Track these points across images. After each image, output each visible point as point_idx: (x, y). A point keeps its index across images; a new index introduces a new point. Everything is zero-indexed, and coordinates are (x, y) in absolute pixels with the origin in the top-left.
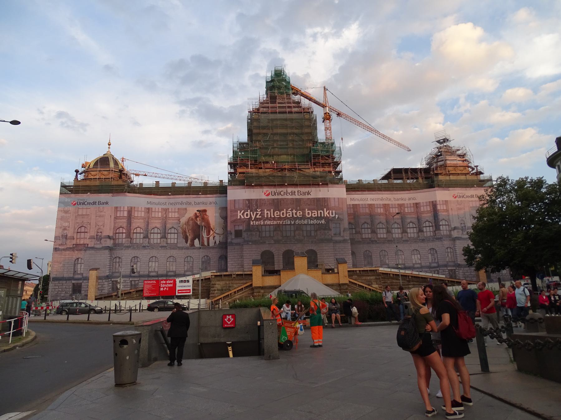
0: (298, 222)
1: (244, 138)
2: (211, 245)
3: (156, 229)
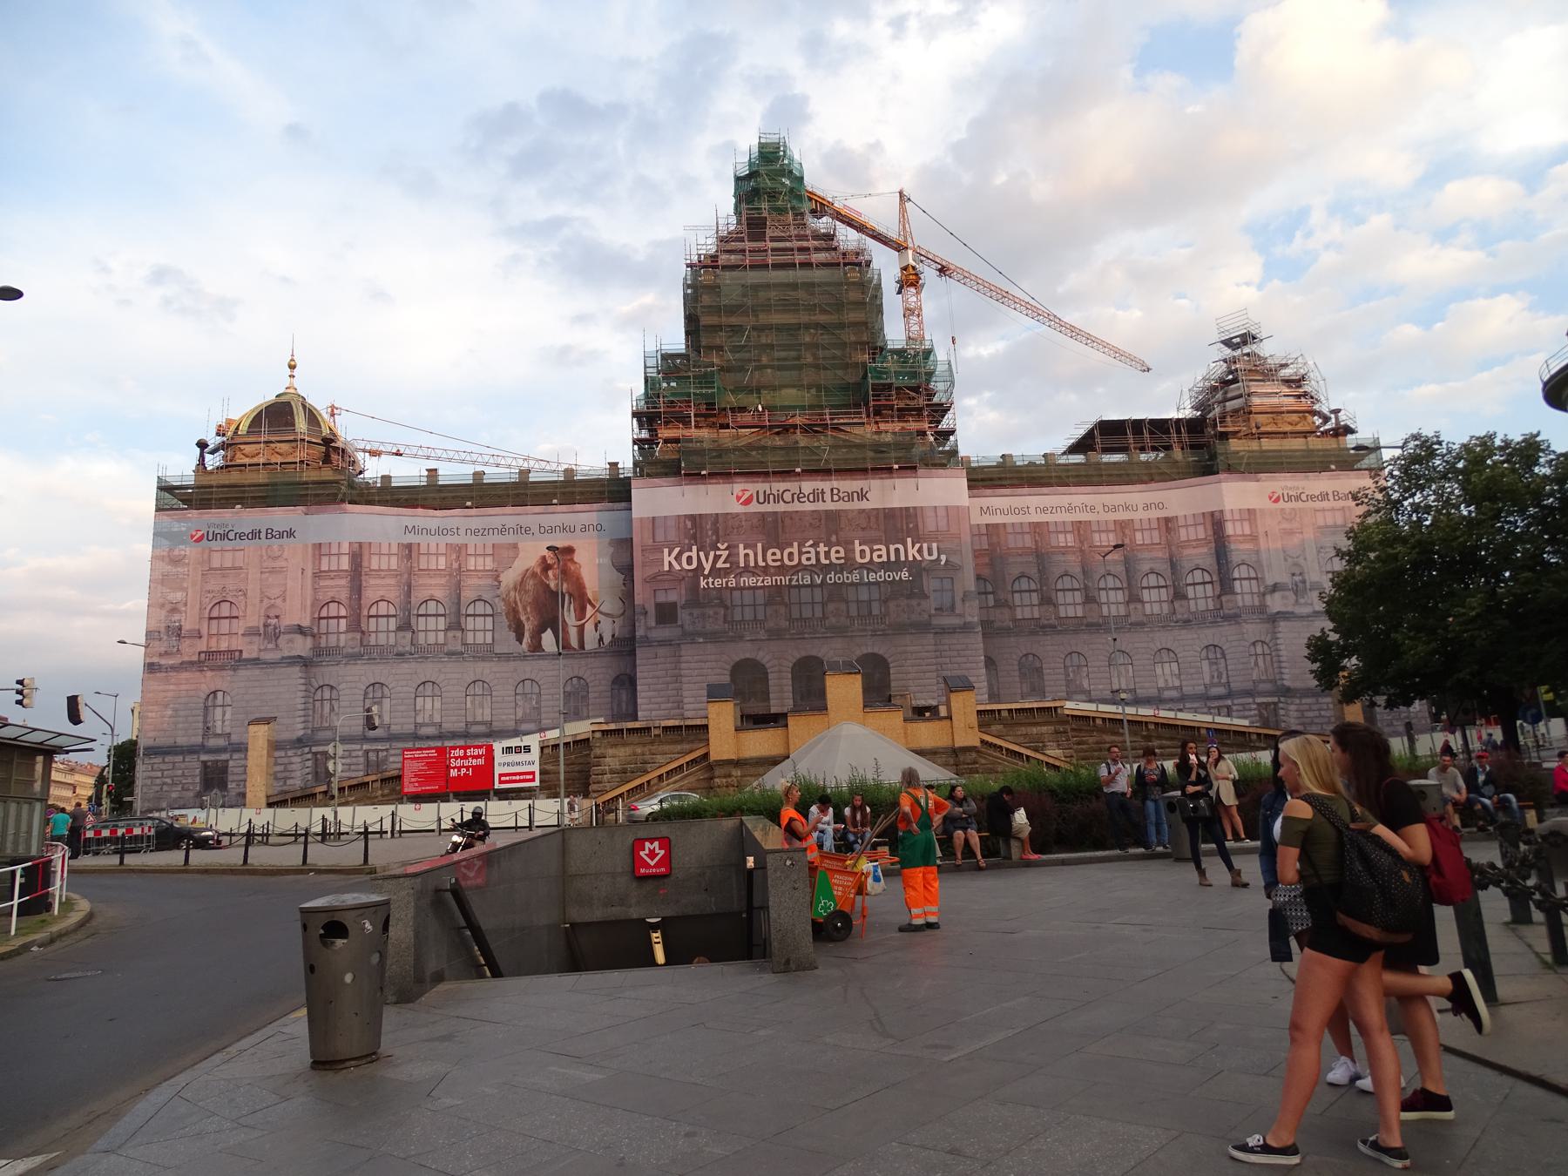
0: (832, 577)
1: (676, 340)
2: (588, 647)
3: (432, 604)
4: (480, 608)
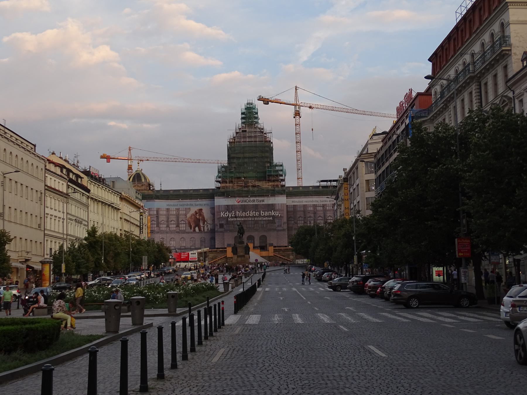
0: (256, 219)
4: (183, 222)
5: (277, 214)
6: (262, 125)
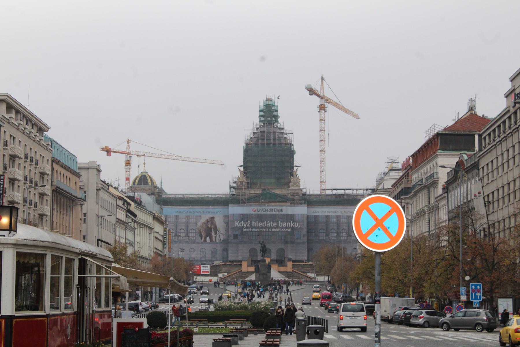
0: (273, 230)
4: (193, 231)
5: (297, 225)
6: (282, 124)
